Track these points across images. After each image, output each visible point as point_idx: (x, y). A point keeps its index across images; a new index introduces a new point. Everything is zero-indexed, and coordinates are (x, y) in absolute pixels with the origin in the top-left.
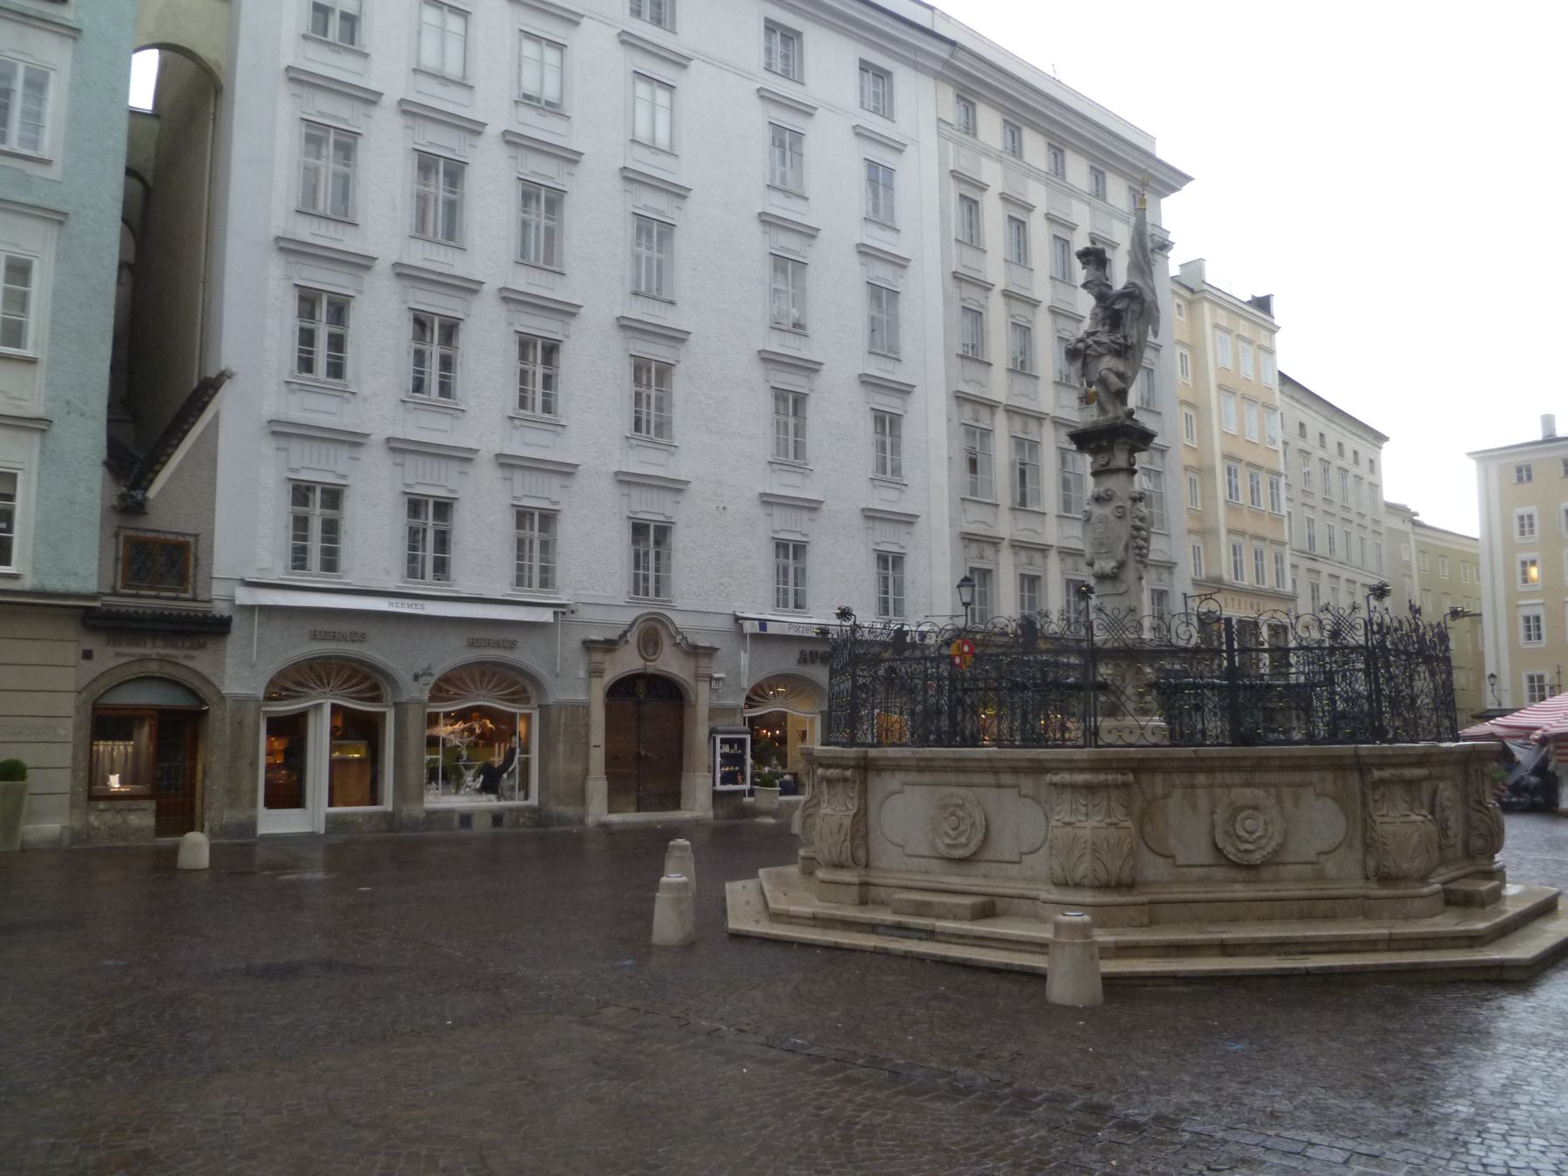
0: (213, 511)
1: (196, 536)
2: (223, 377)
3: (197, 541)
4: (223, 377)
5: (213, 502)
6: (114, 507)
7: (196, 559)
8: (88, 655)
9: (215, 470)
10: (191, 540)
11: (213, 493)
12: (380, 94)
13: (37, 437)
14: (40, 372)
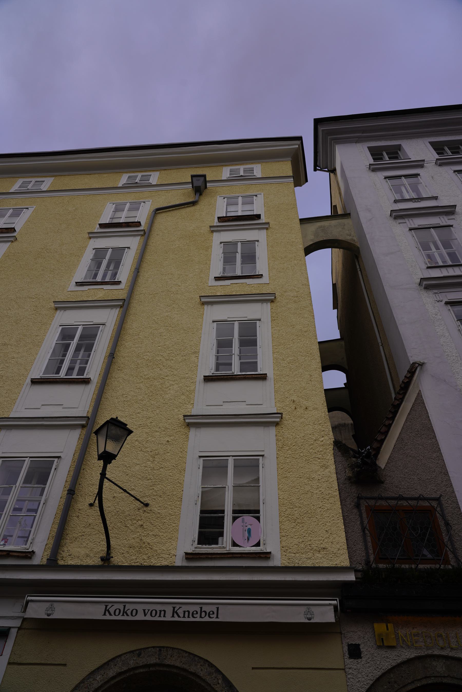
0: (446, 473)
1: (438, 499)
2: (414, 369)
3: (440, 504)
4: (414, 369)
5: (444, 466)
6: (349, 478)
7: (447, 524)
8: (355, 652)
9: (435, 437)
10: (434, 504)
11: (440, 457)
12: (455, 206)
13: (272, 431)
14: (269, 385)
